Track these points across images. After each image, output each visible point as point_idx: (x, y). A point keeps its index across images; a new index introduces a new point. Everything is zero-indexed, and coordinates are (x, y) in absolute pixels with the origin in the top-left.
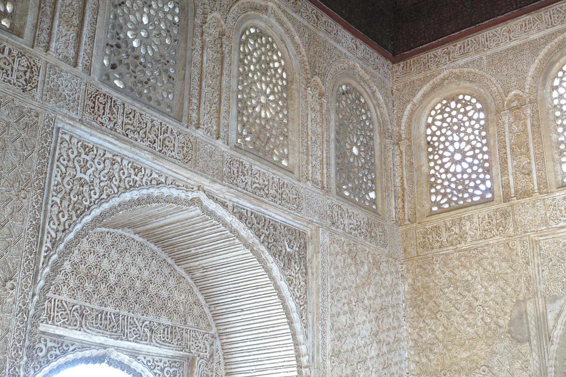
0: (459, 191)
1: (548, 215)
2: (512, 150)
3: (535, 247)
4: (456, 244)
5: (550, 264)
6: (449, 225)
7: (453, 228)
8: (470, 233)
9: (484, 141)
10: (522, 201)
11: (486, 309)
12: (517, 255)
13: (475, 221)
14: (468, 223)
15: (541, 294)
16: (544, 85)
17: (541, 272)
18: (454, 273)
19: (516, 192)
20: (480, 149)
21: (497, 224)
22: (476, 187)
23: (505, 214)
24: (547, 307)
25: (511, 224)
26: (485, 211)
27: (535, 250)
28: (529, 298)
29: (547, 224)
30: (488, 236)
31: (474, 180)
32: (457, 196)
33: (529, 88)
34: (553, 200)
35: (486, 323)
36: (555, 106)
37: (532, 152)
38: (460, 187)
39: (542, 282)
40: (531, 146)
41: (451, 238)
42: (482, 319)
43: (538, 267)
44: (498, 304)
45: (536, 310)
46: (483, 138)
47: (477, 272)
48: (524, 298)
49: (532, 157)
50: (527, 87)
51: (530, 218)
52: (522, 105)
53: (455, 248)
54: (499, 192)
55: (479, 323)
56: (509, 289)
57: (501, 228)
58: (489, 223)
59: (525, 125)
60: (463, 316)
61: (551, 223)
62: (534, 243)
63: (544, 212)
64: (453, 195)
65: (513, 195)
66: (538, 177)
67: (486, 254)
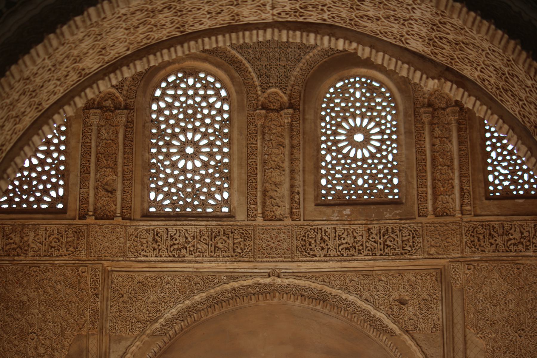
0: (23, 192)
1: (128, 245)
2: (98, 160)
3: (106, 277)
4: (14, 256)
5: (121, 300)
6: (8, 231)
7: (12, 236)
8: (33, 245)
9: (63, 138)
10: (101, 222)
11: (41, 337)
12: (86, 283)
13: (41, 232)
14: (32, 234)
15: (106, 332)
16: (144, 92)
17: (109, 307)
18: (6, 290)
19: (95, 210)
20: (57, 146)
21: (67, 242)
22: (46, 192)
23: (78, 233)
24: (111, 346)
25: (84, 246)
26: (55, 224)
27: (106, 282)
28: (93, 334)
29: (124, 254)
30: (55, 253)
31: (44, 183)
32: (20, 197)
33: (127, 91)
34: (136, 229)
35: (38, 354)
36: (152, 121)
37: (120, 169)
38: (25, 187)
39: (109, 318)
40: (120, 160)
41: (8, 247)
42: (35, 348)
43: (107, 301)
44: (55, 335)
45: (100, 348)
46: (62, 133)
47: (36, 293)
48: (88, 333)
49: (120, 174)
50: (126, 88)
51: (107, 244)
52: (117, 108)
53: (11, 259)
54: (74, 206)
55: (30, 353)
56: (71, 321)
57: (71, 249)
58: (58, 239)
59: (117, 133)
60: (12, 342)
61: (130, 254)
62: (106, 274)
63: (123, 241)
64: (16, 195)
65: (91, 213)
66: (123, 199)
67: (50, 275)
